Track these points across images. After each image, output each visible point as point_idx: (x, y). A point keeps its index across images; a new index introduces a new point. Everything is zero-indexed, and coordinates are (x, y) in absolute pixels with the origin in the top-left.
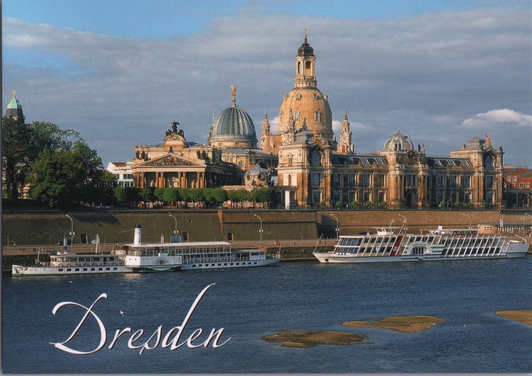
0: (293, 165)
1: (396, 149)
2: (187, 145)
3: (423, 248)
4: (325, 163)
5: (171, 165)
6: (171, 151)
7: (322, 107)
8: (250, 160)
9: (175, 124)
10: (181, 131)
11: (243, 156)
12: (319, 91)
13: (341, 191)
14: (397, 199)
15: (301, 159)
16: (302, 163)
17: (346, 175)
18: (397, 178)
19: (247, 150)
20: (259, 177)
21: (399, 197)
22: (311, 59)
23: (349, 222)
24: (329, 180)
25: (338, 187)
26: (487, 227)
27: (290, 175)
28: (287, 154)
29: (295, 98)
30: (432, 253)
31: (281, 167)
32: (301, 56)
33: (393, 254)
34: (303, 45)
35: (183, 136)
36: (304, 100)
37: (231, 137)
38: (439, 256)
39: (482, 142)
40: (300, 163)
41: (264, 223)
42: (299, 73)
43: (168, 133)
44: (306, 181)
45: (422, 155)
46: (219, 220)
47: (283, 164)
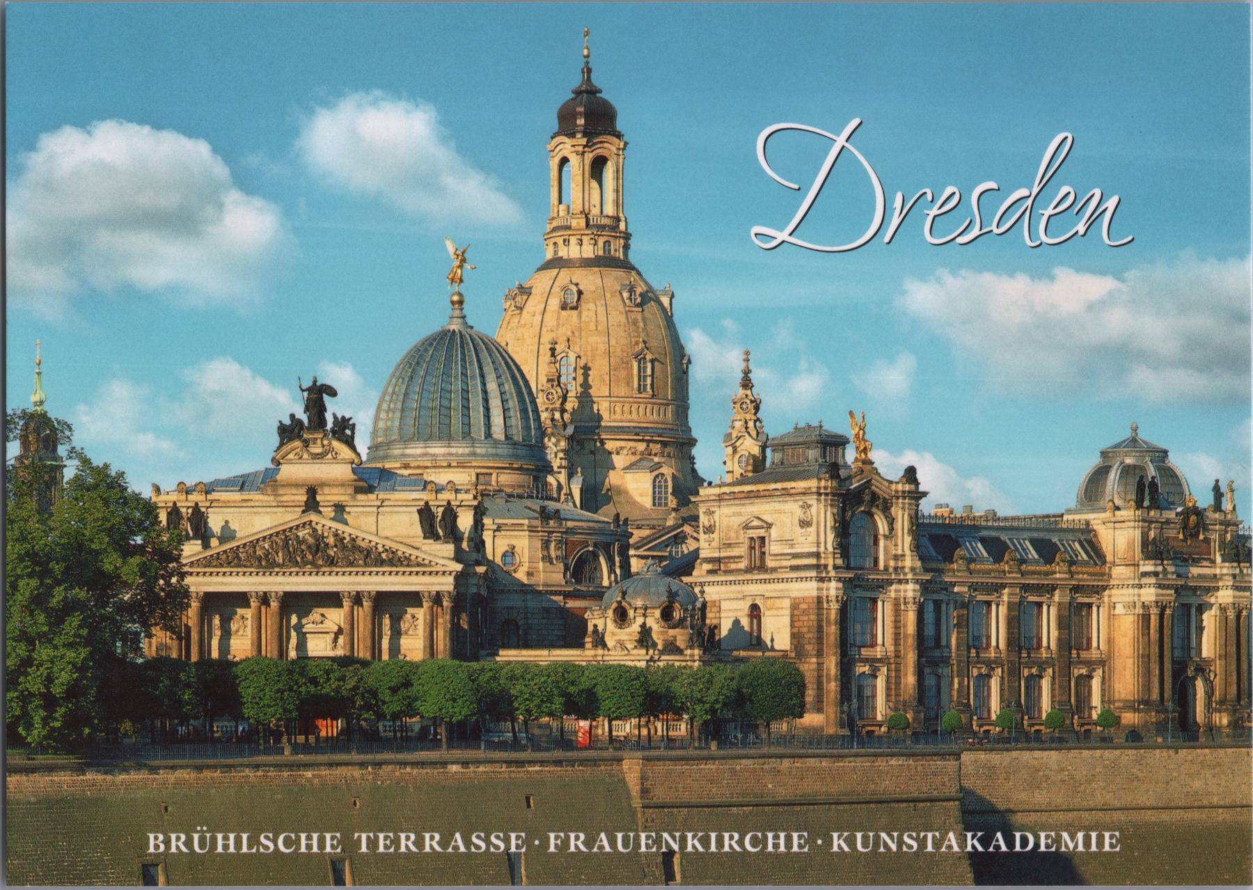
0: (770, 563)
2: (369, 480)
4: (896, 557)
5: (313, 564)
6: (312, 504)
7: (658, 335)
8: (546, 545)
12: (639, 273)
14: (1146, 702)
15: (813, 538)
19: (529, 503)
20: (666, 615)
21: (1155, 695)
22: (609, 147)
23: (1023, 796)
24: (911, 628)
25: (937, 653)
28: (736, 521)
29: (554, 303)
31: (710, 572)
32: (572, 135)
34: (578, 93)
36: (588, 309)
37: (460, 449)
40: (809, 555)
42: (560, 202)
43: (289, 432)
45: (1226, 524)
46: (629, 797)
47: (718, 560)
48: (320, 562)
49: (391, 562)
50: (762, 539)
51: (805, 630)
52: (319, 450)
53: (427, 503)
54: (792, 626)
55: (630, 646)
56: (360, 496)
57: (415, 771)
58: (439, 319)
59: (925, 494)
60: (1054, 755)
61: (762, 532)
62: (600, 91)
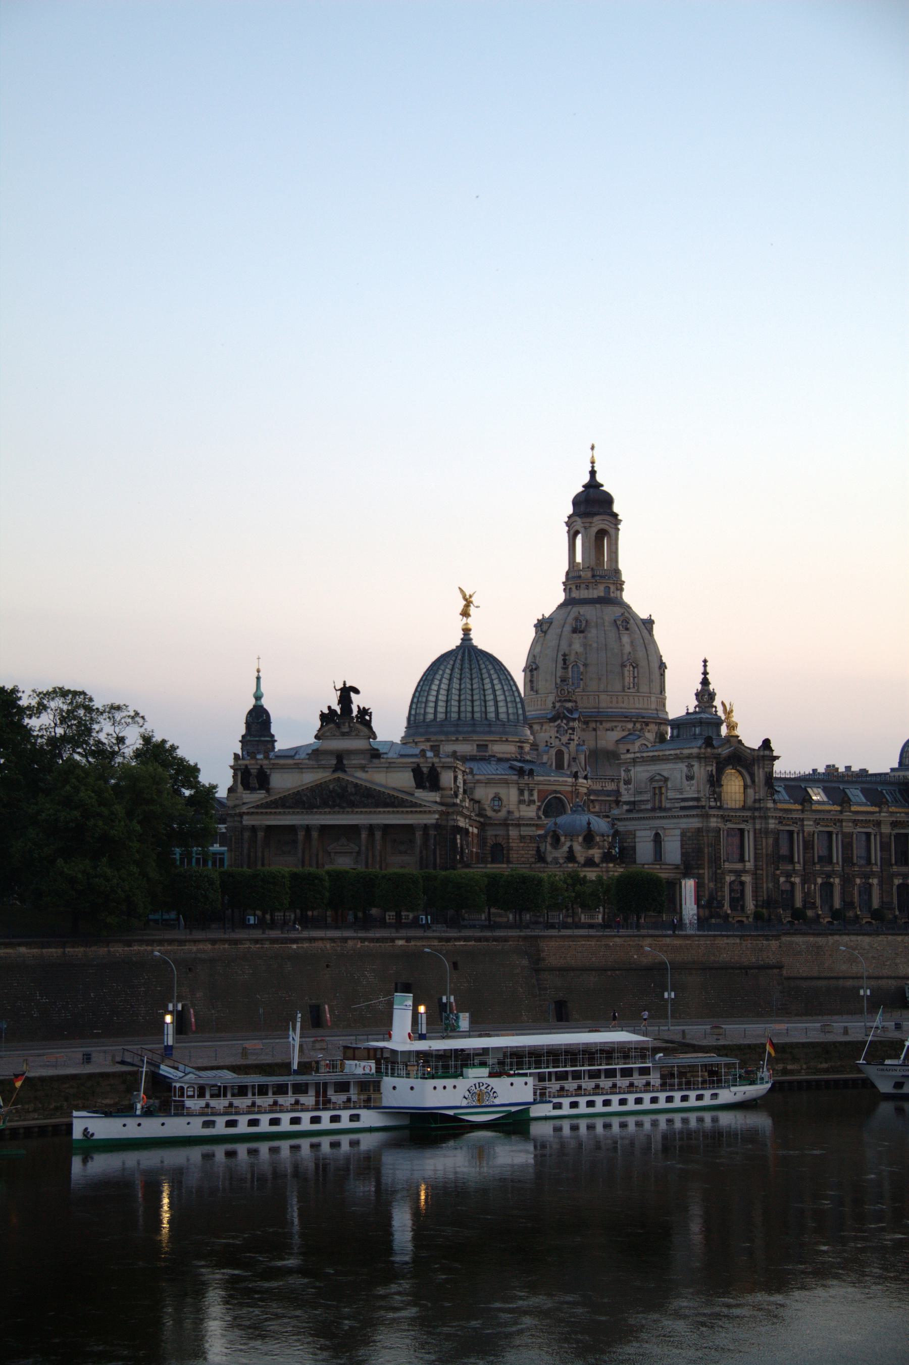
6: (340, 766)
9: (346, 693)
10: (364, 712)
13: (797, 880)
16: (697, 799)
17: (809, 833)
23: (844, 967)
27: (657, 835)
29: (568, 628)
41: (862, 978)
43: (327, 718)
47: (634, 803)
48: (345, 805)
49: (392, 805)
50: (660, 788)
51: (690, 850)
52: (346, 730)
53: (418, 765)
54: (682, 848)
55: (561, 861)
57: (372, 944)
58: (453, 641)
59: (777, 758)
60: (867, 939)
61: (661, 784)
62: (602, 486)
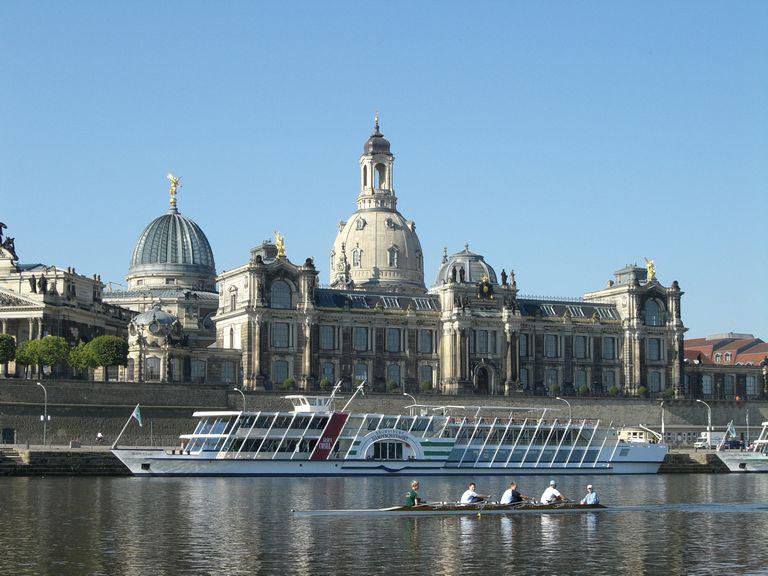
0: (237, 307)
1: (454, 280)
3: (400, 446)
10: (10, 241)
11: (172, 303)
13: (337, 362)
17: (347, 328)
18: (455, 335)
26: (632, 432)
27: (232, 330)
30: (424, 457)
32: (366, 155)
33: (320, 456)
35: (12, 251)
37: (158, 267)
38: (442, 464)
39: (640, 274)
44: (257, 337)
56: (13, 275)
